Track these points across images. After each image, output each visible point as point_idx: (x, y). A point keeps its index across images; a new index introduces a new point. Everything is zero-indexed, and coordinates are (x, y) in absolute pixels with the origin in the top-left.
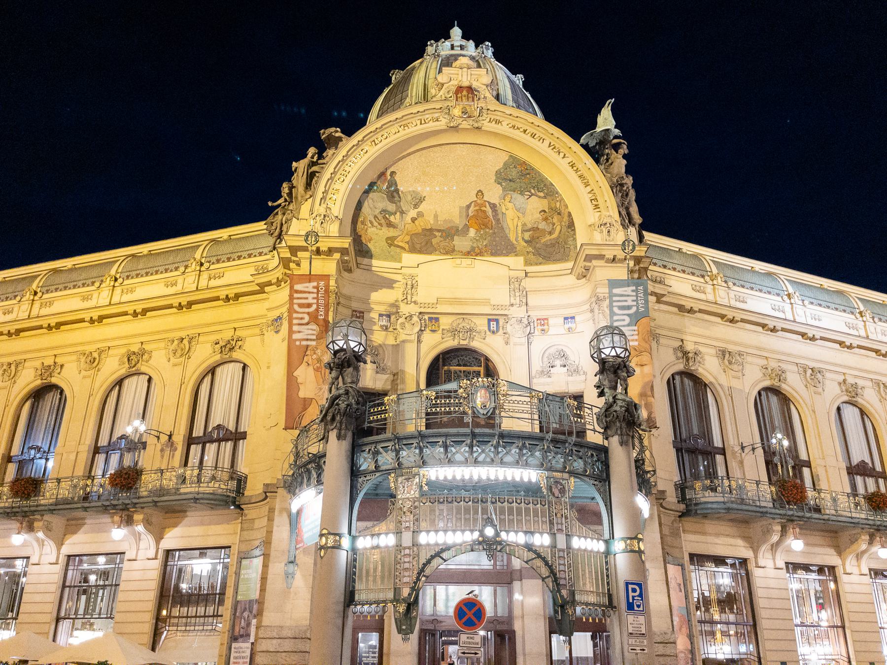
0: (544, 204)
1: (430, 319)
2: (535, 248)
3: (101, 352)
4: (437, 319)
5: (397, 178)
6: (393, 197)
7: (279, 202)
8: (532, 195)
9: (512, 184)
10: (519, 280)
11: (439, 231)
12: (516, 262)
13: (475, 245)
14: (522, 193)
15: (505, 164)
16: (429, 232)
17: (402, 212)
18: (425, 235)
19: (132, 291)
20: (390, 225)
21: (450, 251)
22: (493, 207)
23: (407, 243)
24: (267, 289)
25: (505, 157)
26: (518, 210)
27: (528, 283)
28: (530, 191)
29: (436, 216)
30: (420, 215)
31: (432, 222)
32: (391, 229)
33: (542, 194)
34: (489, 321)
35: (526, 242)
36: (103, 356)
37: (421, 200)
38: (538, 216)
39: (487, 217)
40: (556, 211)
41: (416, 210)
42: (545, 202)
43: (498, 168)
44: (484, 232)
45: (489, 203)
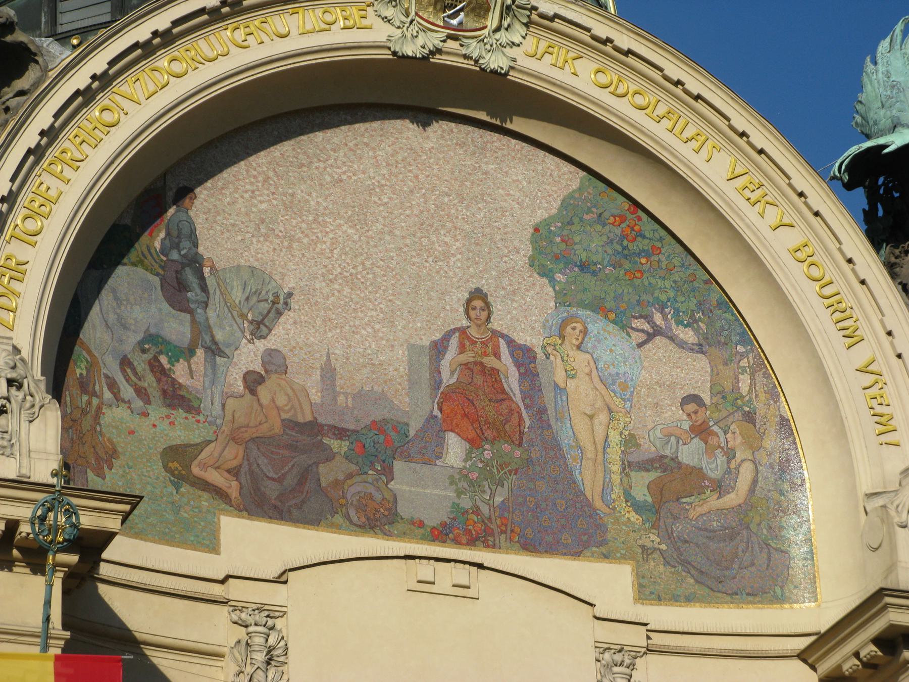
0: (696, 374)
2: (670, 536)
6: (182, 286)
8: (657, 332)
9: (588, 280)
11: (341, 433)
12: (610, 583)
13: (466, 503)
15: (566, 204)
16: (306, 436)
18: (293, 447)
20: (177, 398)
21: (378, 518)
22: (524, 357)
23: (234, 472)
28: (648, 318)
29: (329, 373)
30: (275, 363)
31: (316, 396)
32: (180, 414)
33: (688, 336)
35: (638, 507)
37: (279, 305)
38: (675, 415)
39: (500, 394)
41: (261, 345)
42: (702, 362)
43: (541, 215)
45: (510, 342)
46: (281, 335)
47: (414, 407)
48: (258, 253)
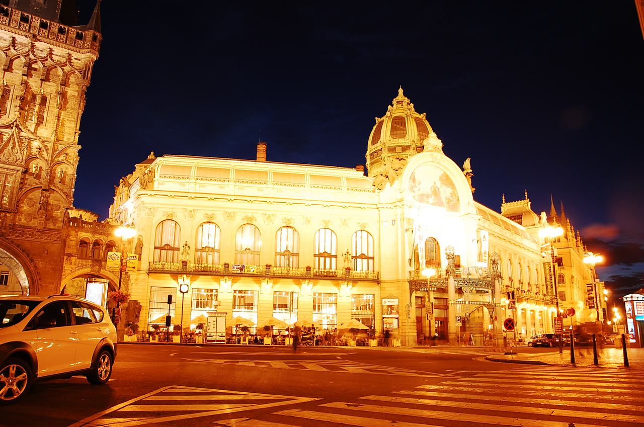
20: (414, 192)
22: (438, 188)
25: (442, 172)
37: (420, 183)
38: (450, 195)
40: (454, 194)
47: (430, 192)
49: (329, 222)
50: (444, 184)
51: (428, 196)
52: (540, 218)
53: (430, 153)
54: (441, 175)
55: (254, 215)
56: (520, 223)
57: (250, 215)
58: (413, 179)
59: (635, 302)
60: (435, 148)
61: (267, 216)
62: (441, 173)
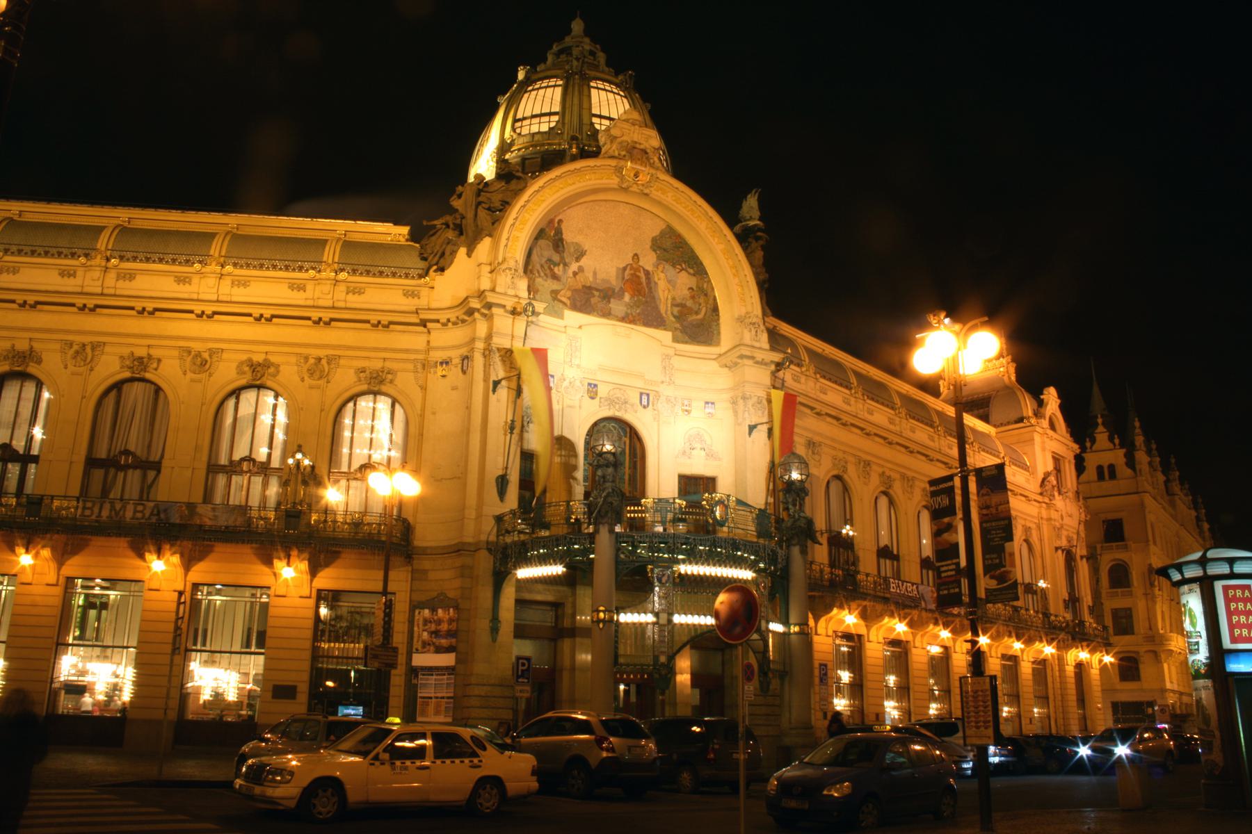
1: (590, 384)
3: (212, 352)
4: (596, 386)
5: (563, 226)
7: (435, 222)
10: (668, 357)
11: (597, 290)
14: (674, 266)
16: (588, 290)
17: (565, 265)
19: (245, 284)
21: (606, 314)
22: (647, 273)
24: (429, 325)
26: (669, 282)
27: (677, 362)
29: (595, 273)
30: (581, 269)
34: (641, 394)
36: (215, 359)
38: (686, 293)
39: (640, 284)
40: (703, 291)
42: (694, 279)
44: (632, 299)
46: (584, 262)
47: (615, 283)
48: (579, 239)
49: (266, 365)
50: (667, 261)
51: (608, 294)
52: (1041, 403)
53: (613, 163)
54: (656, 233)
55: (36, 346)
56: (985, 418)
57: (22, 346)
58: (550, 236)
59: (1219, 586)
60: (634, 152)
61: (75, 347)
62: (653, 228)
